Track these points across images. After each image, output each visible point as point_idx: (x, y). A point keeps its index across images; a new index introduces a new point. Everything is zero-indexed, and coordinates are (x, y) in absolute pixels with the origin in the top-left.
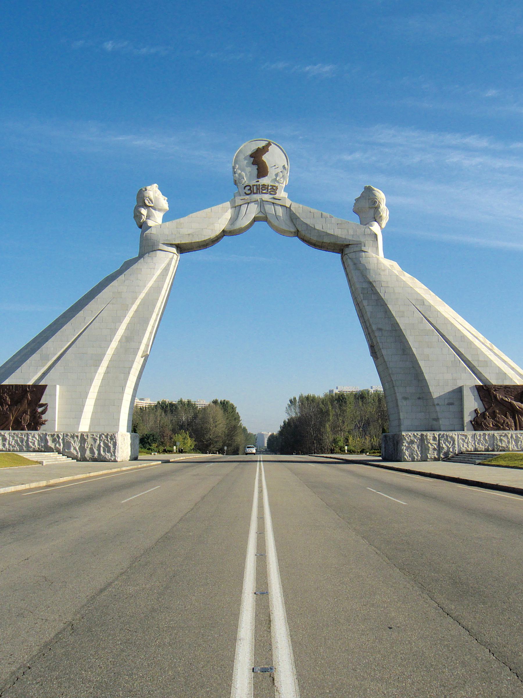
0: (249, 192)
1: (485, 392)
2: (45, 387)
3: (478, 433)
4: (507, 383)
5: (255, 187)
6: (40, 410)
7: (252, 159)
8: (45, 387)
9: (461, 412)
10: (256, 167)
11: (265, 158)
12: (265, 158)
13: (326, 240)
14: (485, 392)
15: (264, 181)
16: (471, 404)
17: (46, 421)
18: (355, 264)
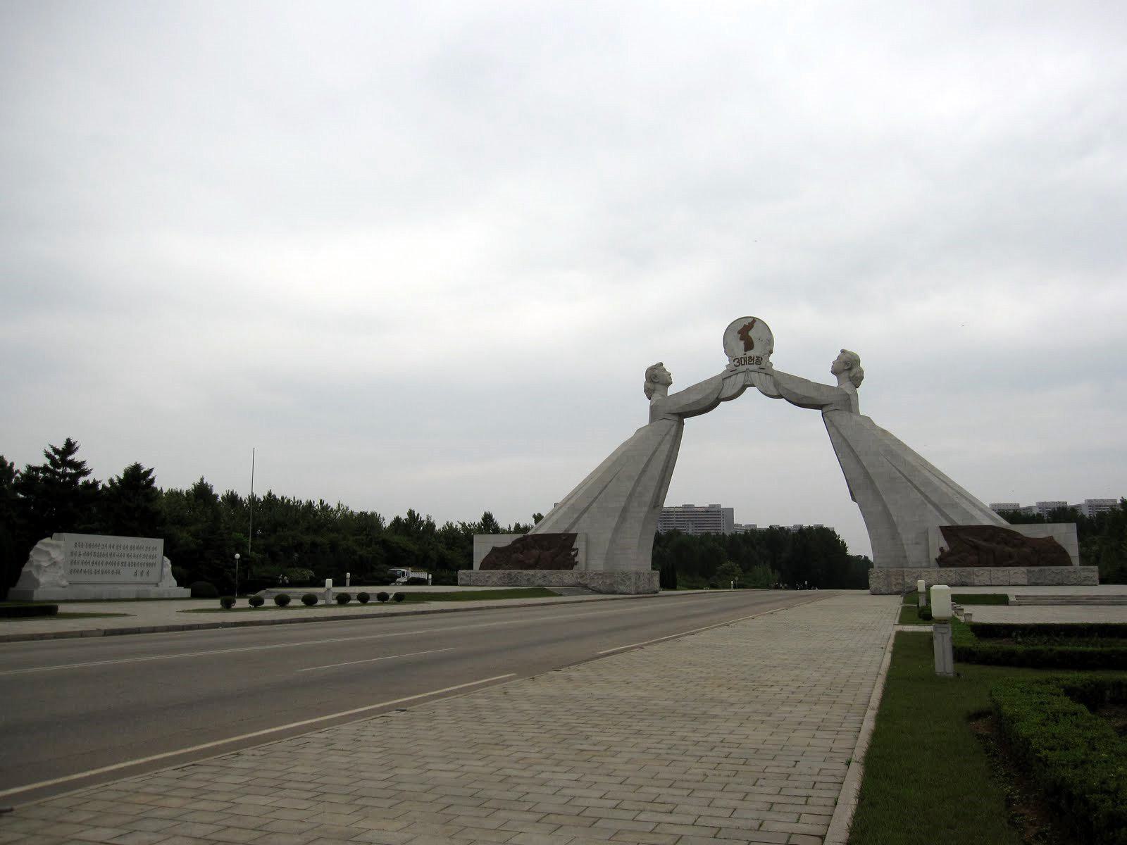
0: (738, 364)
1: (950, 532)
2: (575, 535)
3: (943, 569)
4: (973, 524)
5: (743, 360)
6: (573, 553)
7: (740, 335)
8: (575, 535)
9: (928, 551)
10: (743, 342)
11: (752, 334)
12: (752, 334)
13: (804, 402)
14: (950, 532)
15: (751, 353)
16: (939, 543)
17: (577, 562)
18: (831, 421)
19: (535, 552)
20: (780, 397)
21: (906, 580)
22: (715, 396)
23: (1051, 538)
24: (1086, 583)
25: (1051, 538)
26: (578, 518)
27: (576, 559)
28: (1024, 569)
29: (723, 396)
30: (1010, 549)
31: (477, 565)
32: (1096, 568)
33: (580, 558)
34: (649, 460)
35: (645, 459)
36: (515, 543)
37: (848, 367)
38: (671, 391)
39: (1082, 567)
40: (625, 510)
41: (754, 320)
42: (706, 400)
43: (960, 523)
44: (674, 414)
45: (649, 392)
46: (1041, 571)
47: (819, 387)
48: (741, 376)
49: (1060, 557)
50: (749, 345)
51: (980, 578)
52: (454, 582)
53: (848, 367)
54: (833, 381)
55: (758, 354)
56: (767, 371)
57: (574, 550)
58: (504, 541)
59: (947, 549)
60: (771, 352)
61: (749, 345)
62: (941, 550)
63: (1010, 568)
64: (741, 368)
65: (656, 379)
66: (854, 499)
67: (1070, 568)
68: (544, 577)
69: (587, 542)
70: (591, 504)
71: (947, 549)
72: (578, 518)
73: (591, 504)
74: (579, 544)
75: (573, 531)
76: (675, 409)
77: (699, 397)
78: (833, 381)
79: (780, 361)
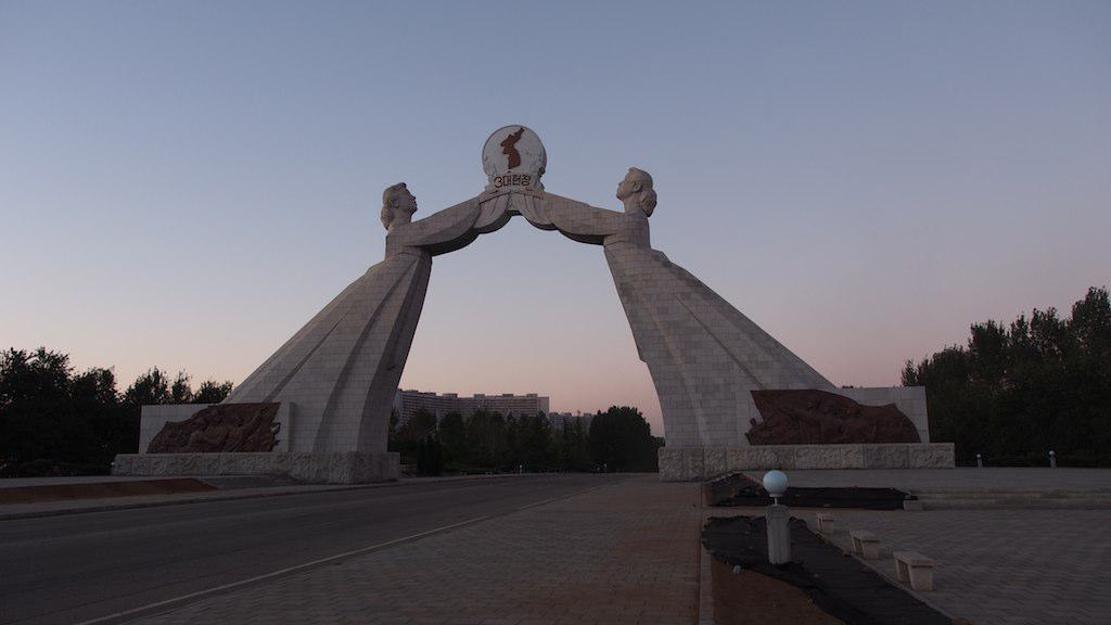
1: (762, 398)
6: (273, 429)
10: (507, 156)
11: (517, 146)
12: (517, 146)
13: (582, 232)
14: (762, 398)
15: (516, 171)
16: (746, 412)
19: (221, 429)
20: (551, 227)
21: (707, 462)
22: (470, 224)
23: (894, 406)
24: (939, 465)
25: (894, 406)
26: (285, 381)
27: (277, 437)
28: (858, 447)
29: (478, 226)
30: (840, 421)
31: (143, 447)
32: (953, 444)
33: (283, 436)
34: (381, 306)
35: (375, 305)
36: (197, 416)
37: (640, 191)
38: (415, 217)
39: (933, 444)
40: (347, 371)
41: (522, 130)
42: (460, 231)
43: (776, 387)
44: (416, 247)
45: (388, 218)
46: (880, 449)
47: (598, 213)
48: (503, 199)
49: (906, 432)
50: (515, 160)
51: (803, 459)
52: (108, 472)
53: (640, 191)
54: (619, 207)
55: (526, 172)
56: (538, 193)
57: (275, 425)
58: (184, 413)
59: (760, 420)
60: (542, 171)
61: (515, 160)
62: (753, 421)
63: (840, 445)
64: (505, 189)
65: (398, 202)
66: (642, 358)
67: (916, 445)
68: (231, 461)
69: (295, 411)
70: (302, 363)
71: (760, 420)
72: (285, 381)
73: (302, 363)
74: (283, 417)
75: (274, 401)
76: (418, 239)
77: (449, 225)
78: (619, 207)
79: (552, 183)
